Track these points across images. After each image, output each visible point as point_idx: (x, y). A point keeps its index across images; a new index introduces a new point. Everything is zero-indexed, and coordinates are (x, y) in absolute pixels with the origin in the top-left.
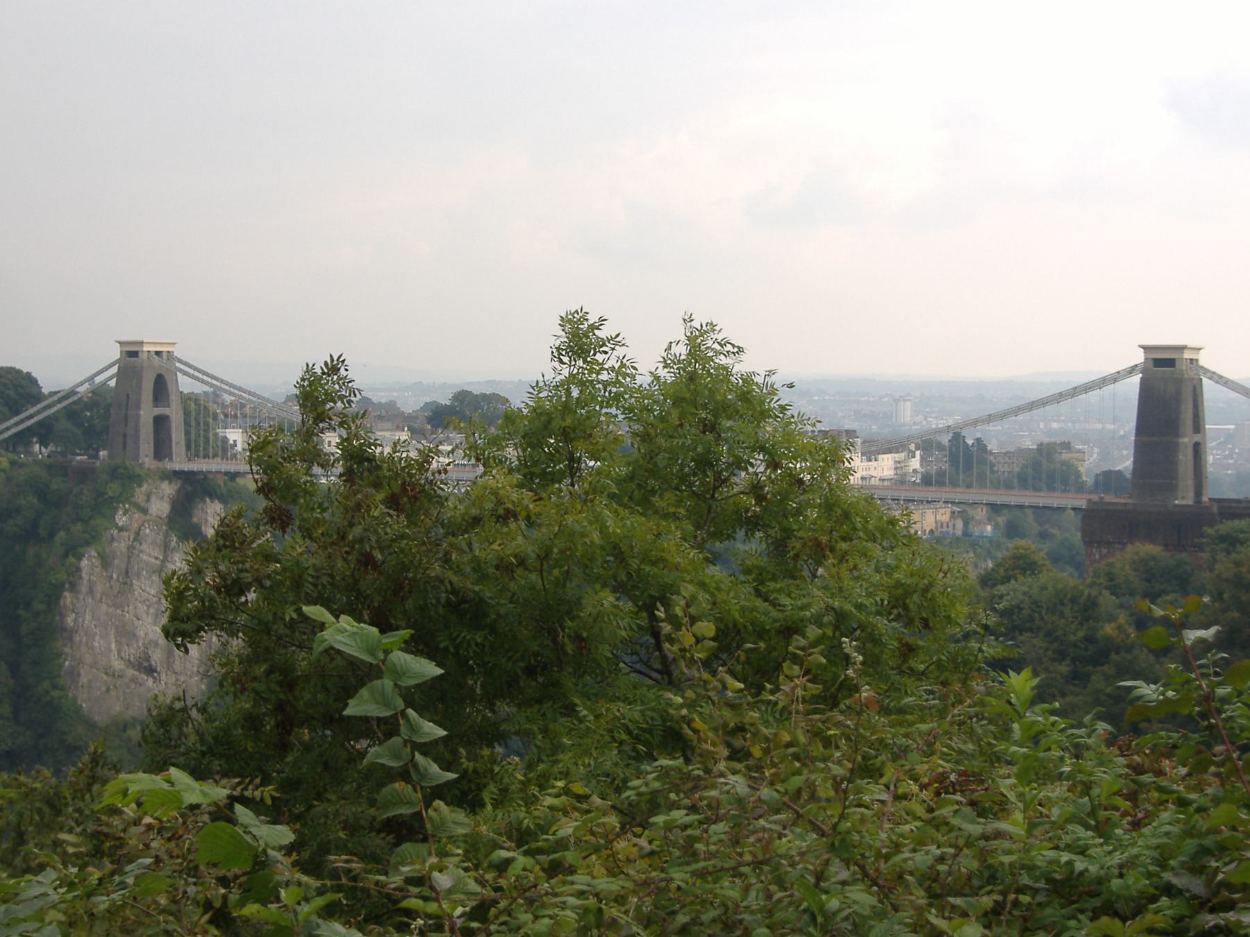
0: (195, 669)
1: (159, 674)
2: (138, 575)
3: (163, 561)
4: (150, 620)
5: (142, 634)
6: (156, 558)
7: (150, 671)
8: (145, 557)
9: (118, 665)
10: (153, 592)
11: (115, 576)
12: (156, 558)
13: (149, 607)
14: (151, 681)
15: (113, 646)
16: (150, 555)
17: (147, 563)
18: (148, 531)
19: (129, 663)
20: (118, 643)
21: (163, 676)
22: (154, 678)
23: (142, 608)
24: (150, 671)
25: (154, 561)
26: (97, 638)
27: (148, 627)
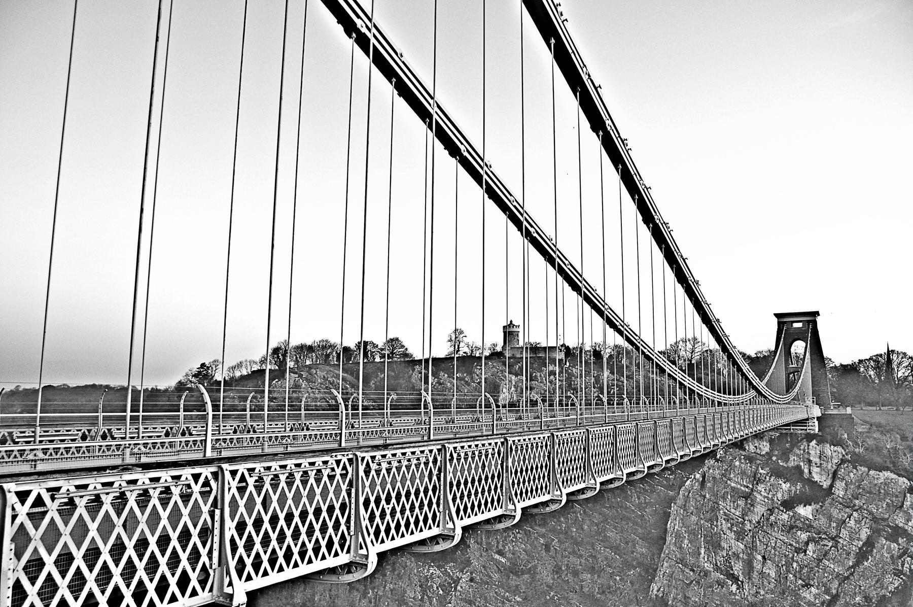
0: (772, 586)
1: (742, 582)
2: (724, 498)
3: (752, 490)
4: (732, 535)
5: (725, 546)
6: (747, 487)
7: (735, 579)
8: (733, 485)
9: (708, 566)
10: (737, 513)
11: (707, 496)
12: (747, 487)
13: (732, 525)
14: (734, 588)
15: (703, 551)
16: (737, 483)
17: (733, 489)
18: (737, 463)
19: (717, 568)
20: (707, 549)
21: (746, 586)
22: (738, 585)
23: (725, 526)
24: (735, 579)
25: (743, 488)
26: (686, 541)
27: (733, 541)
